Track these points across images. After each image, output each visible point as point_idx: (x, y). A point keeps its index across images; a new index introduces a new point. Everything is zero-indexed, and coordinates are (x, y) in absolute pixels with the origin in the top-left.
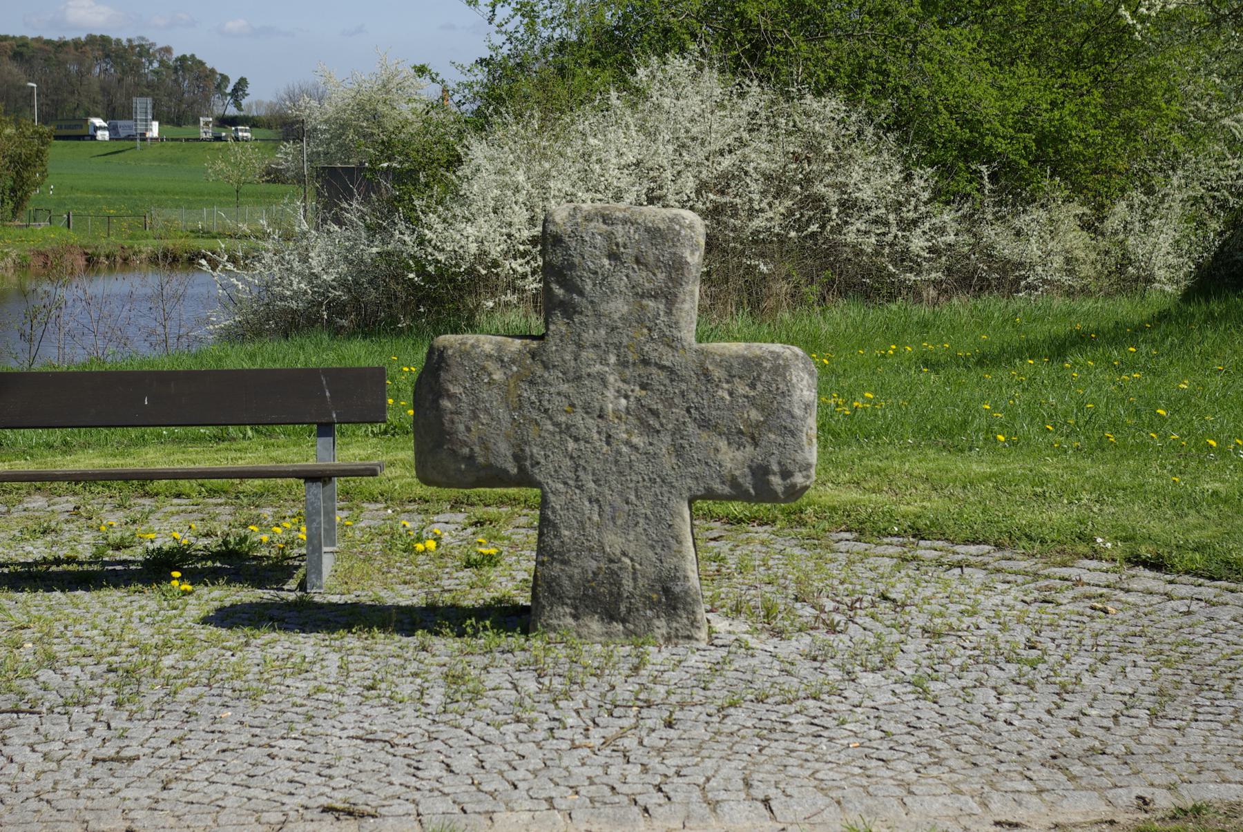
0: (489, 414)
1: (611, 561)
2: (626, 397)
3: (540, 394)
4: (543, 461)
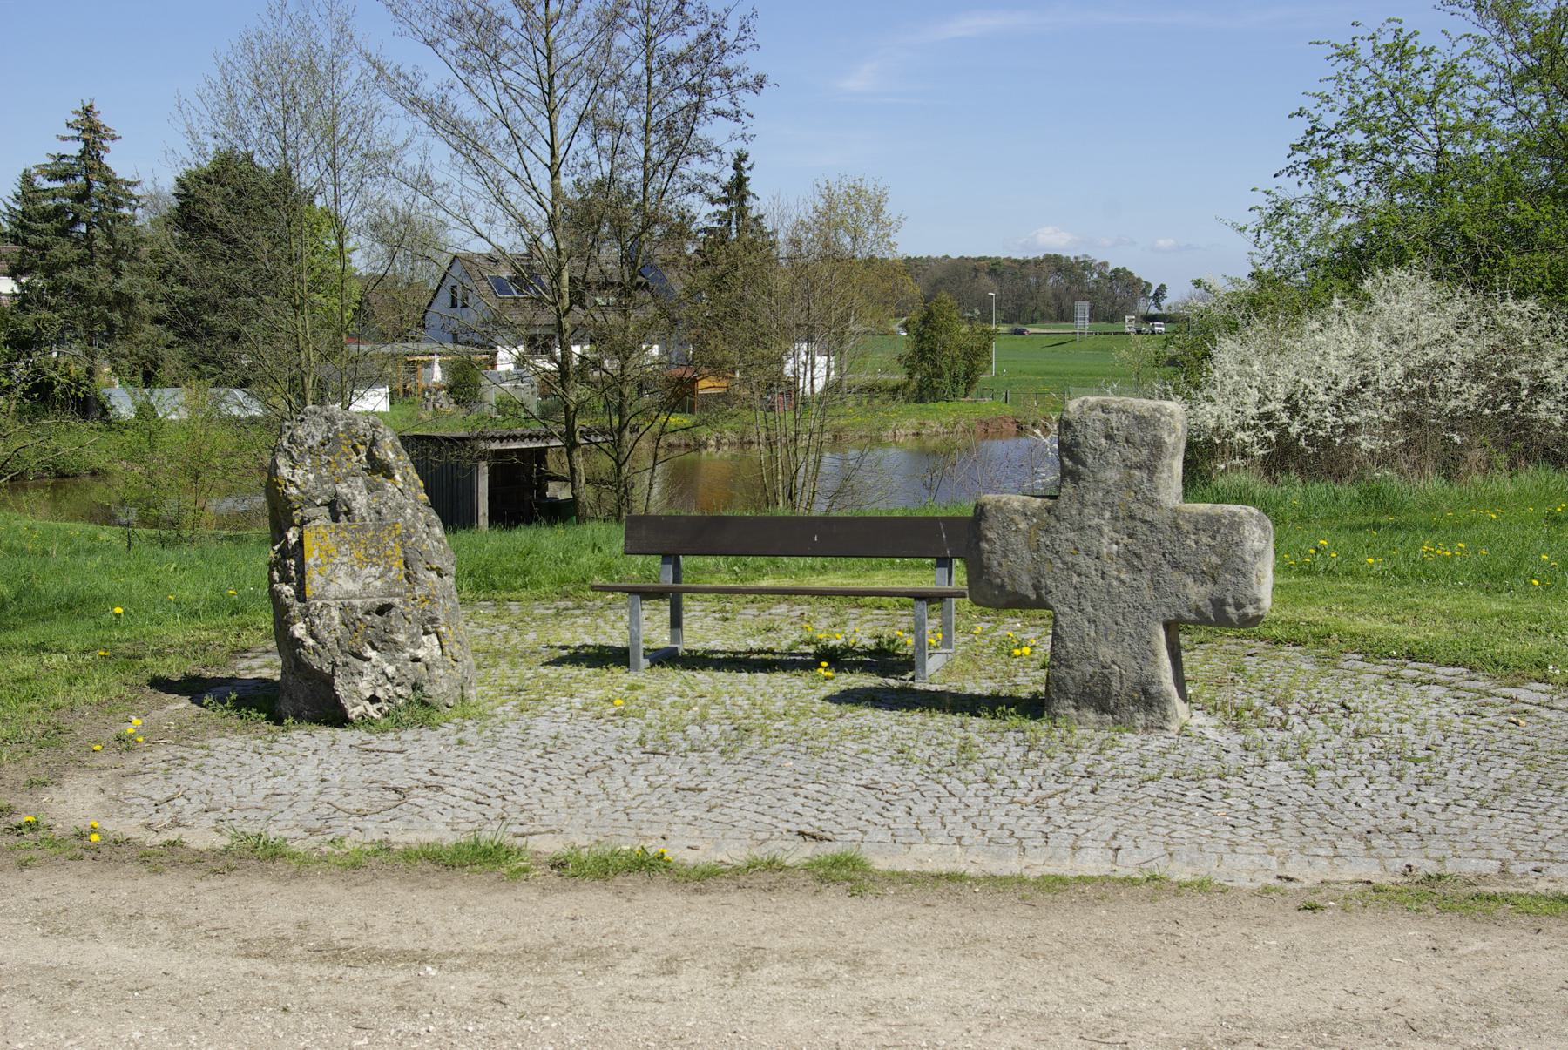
1: (1104, 667)
2: (1117, 543)
3: (1053, 540)
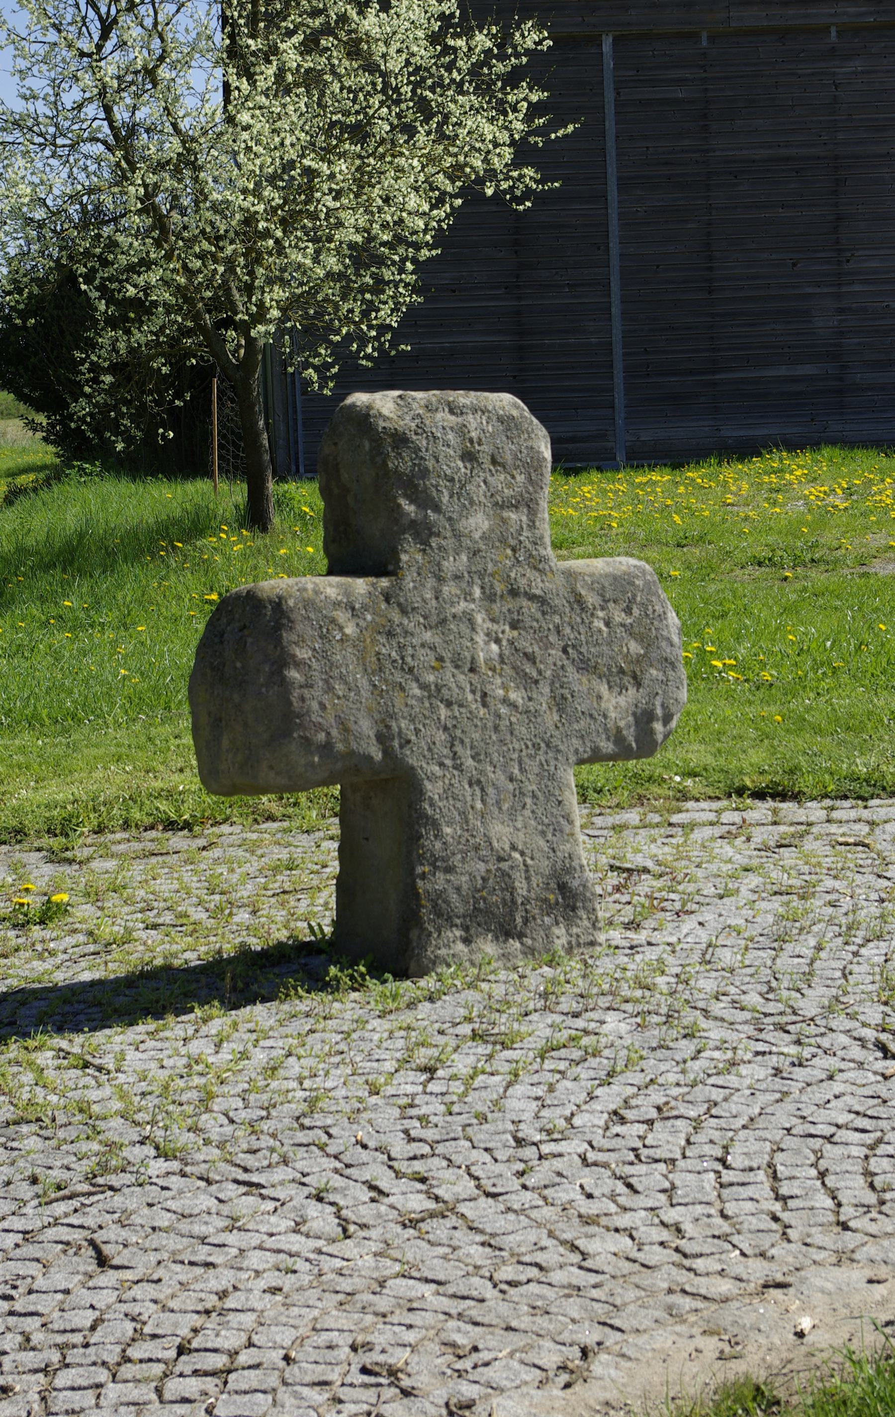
0: (346, 683)
1: (500, 859)
2: (498, 641)
3: (401, 648)
4: (413, 738)
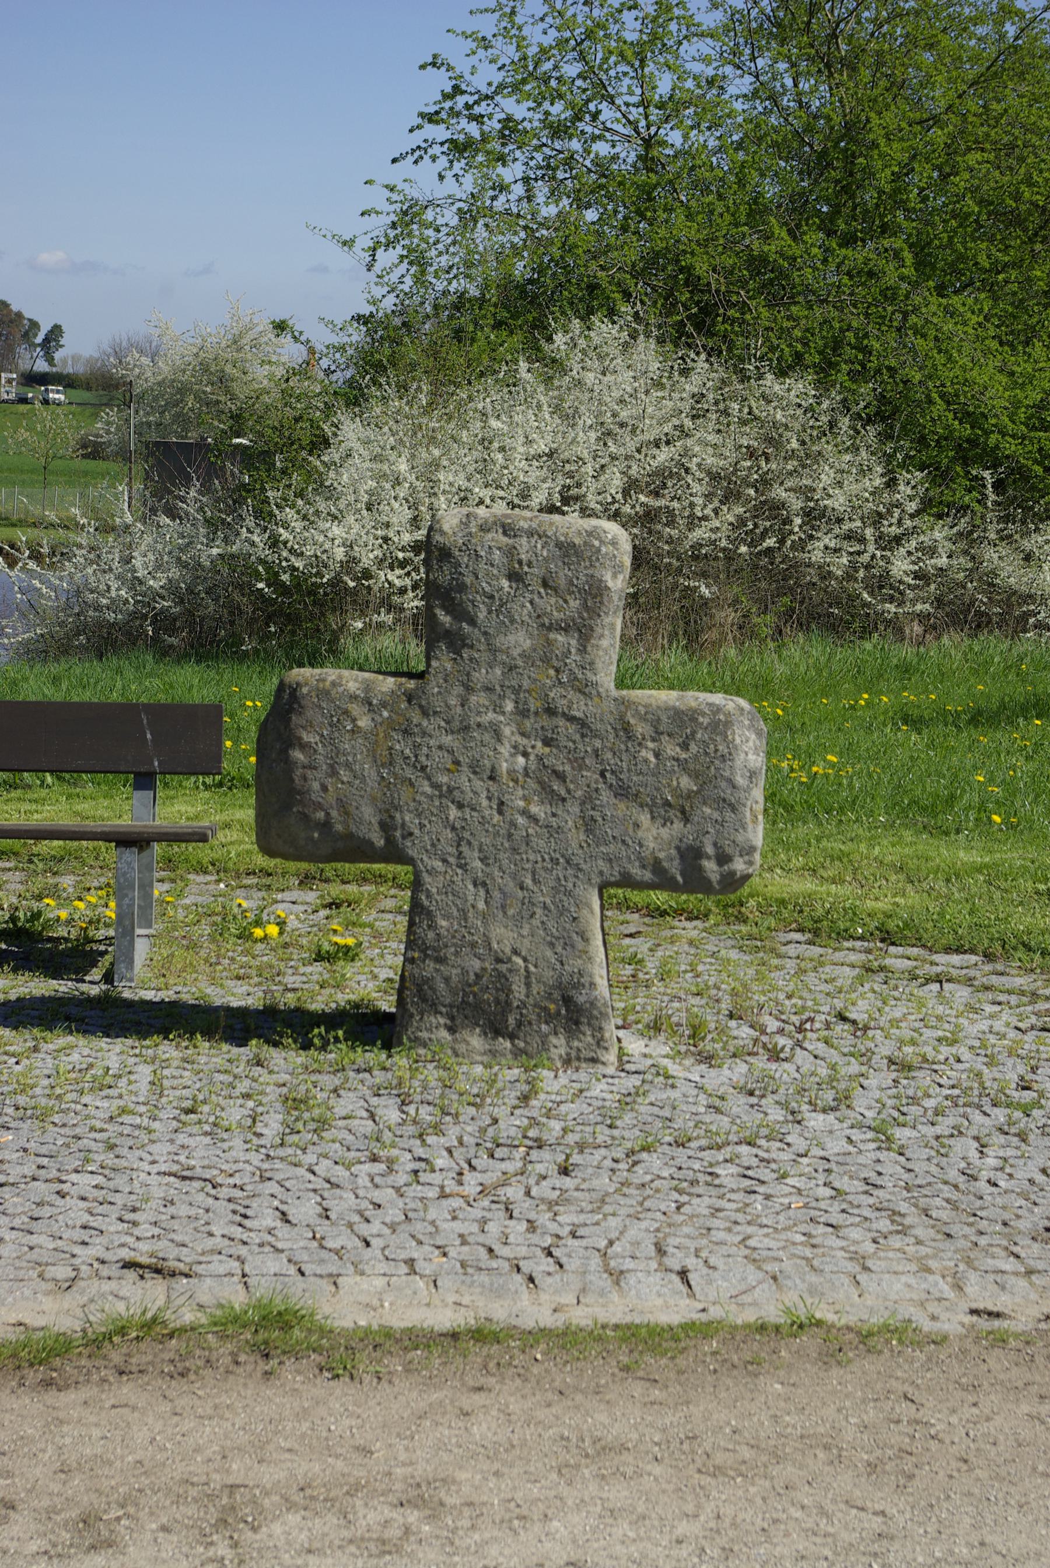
0: (351, 770)
1: (499, 960)
2: (525, 754)
3: (416, 747)
4: (417, 832)
